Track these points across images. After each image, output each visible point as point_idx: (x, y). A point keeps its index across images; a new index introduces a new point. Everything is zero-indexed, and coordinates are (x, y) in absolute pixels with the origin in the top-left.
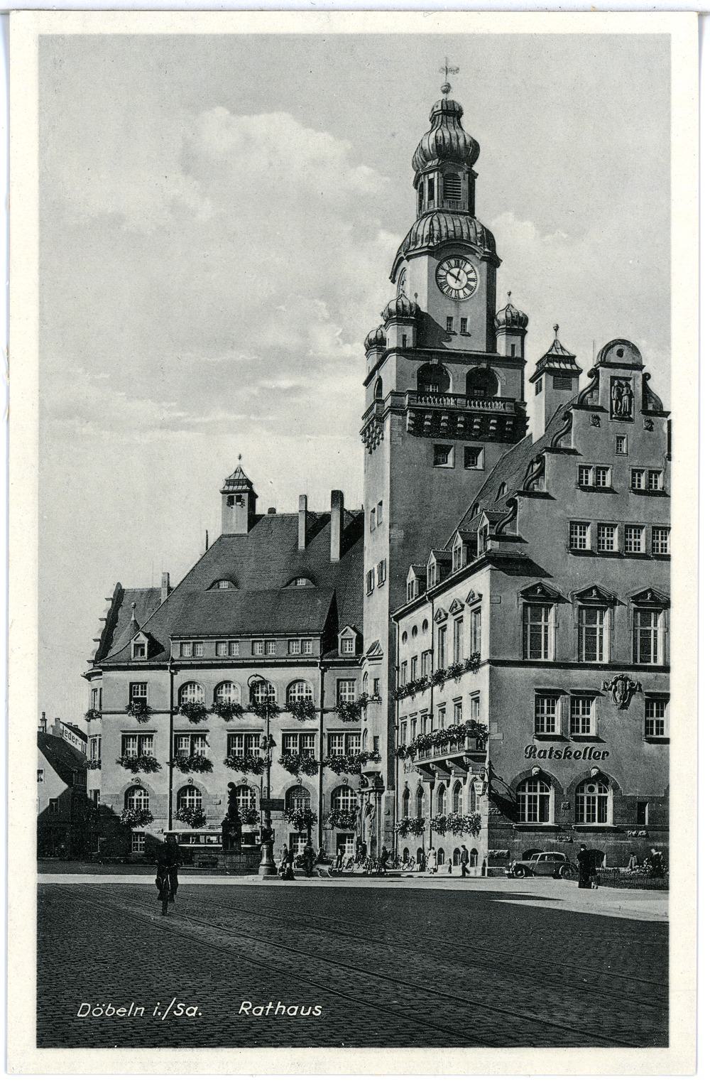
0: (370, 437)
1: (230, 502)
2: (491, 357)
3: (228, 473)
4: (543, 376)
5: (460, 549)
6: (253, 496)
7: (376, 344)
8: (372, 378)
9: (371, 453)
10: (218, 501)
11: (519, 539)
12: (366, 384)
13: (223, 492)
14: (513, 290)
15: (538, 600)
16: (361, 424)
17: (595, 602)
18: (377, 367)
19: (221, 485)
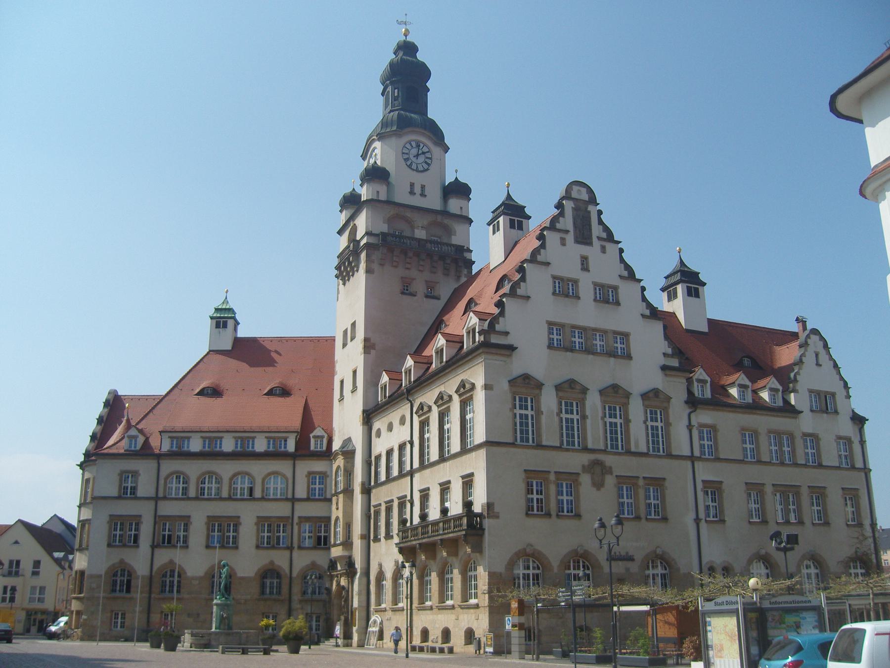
0: (345, 269)
1: (218, 326)
2: (445, 213)
3: (218, 304)
4: (501, 219)
5: (474, 330)
6: (237, 323)
7: (351, 202)
8: (348, 226)
9: (344, 284)
10: (208, 324)
11: (507, 333)
12: (340, 232)
13: (212, 318)
14: (456, 166)
15: (525, 387)
16: (336, 262)
17: (571, 390)
18: (352, 218)
19: (212, 312)
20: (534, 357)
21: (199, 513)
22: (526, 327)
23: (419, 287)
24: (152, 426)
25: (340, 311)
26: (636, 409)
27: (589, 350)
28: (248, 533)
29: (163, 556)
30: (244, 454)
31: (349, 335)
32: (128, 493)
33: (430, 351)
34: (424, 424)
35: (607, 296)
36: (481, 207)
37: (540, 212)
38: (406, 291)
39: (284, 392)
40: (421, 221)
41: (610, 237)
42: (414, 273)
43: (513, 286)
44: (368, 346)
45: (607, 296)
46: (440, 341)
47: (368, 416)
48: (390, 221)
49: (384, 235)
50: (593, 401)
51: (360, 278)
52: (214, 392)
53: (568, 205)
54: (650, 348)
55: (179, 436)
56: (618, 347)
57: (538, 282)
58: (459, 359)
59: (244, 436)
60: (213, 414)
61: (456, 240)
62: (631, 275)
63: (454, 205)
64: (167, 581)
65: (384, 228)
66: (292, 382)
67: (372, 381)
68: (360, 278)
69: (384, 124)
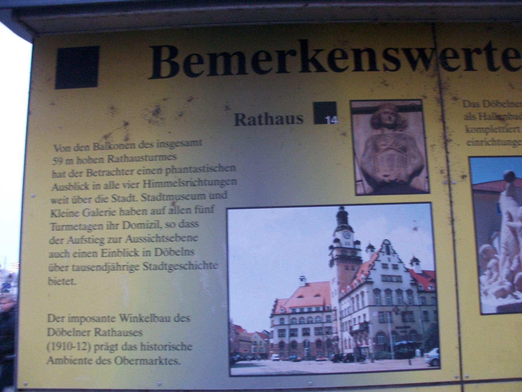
2: (355, 249)
20: (378, 283)
21: (300, 328)
22: (376, 276)
23: (350, 268)
24: (287, 306)
25: (331, 275)
26: (405, 295)
27: (392, 281)
28: (312, 332)
29: (293, 339)
30: (310, 312)
31: (333, 280)
32: (282, 324)
33: (353, 284)
34: (353, 302)
35: (395, 267)
36: (363, 246)
37: (378, 247)
38: (347, 269)
39: (318, 295)
40: (349, 251)
41: (395, 253)
42: (348, 264)
43: (372, 267)
44: (339, 283)
45: (395, 267)
46: (355, 281)
47: (340, 300)
48: (342, 252)
49: (339, 256)
50: (394, 294)
51: (335, 267)
52: (301, 297)
53: (384, 246)
54: (407, 279)
55: (294, 309)
56: (399, 279)
57: (378, 265)
58: (361, 286)
59: (310, 308)
60: (301, 303)
61: (358, 255)
62: (401, 262)
63: (357, 247)
64: (294, 344)
65: (339, 254)
66: (320, 293)
67: (340, 292)
68: (335, 267)
69: (338, 227)
